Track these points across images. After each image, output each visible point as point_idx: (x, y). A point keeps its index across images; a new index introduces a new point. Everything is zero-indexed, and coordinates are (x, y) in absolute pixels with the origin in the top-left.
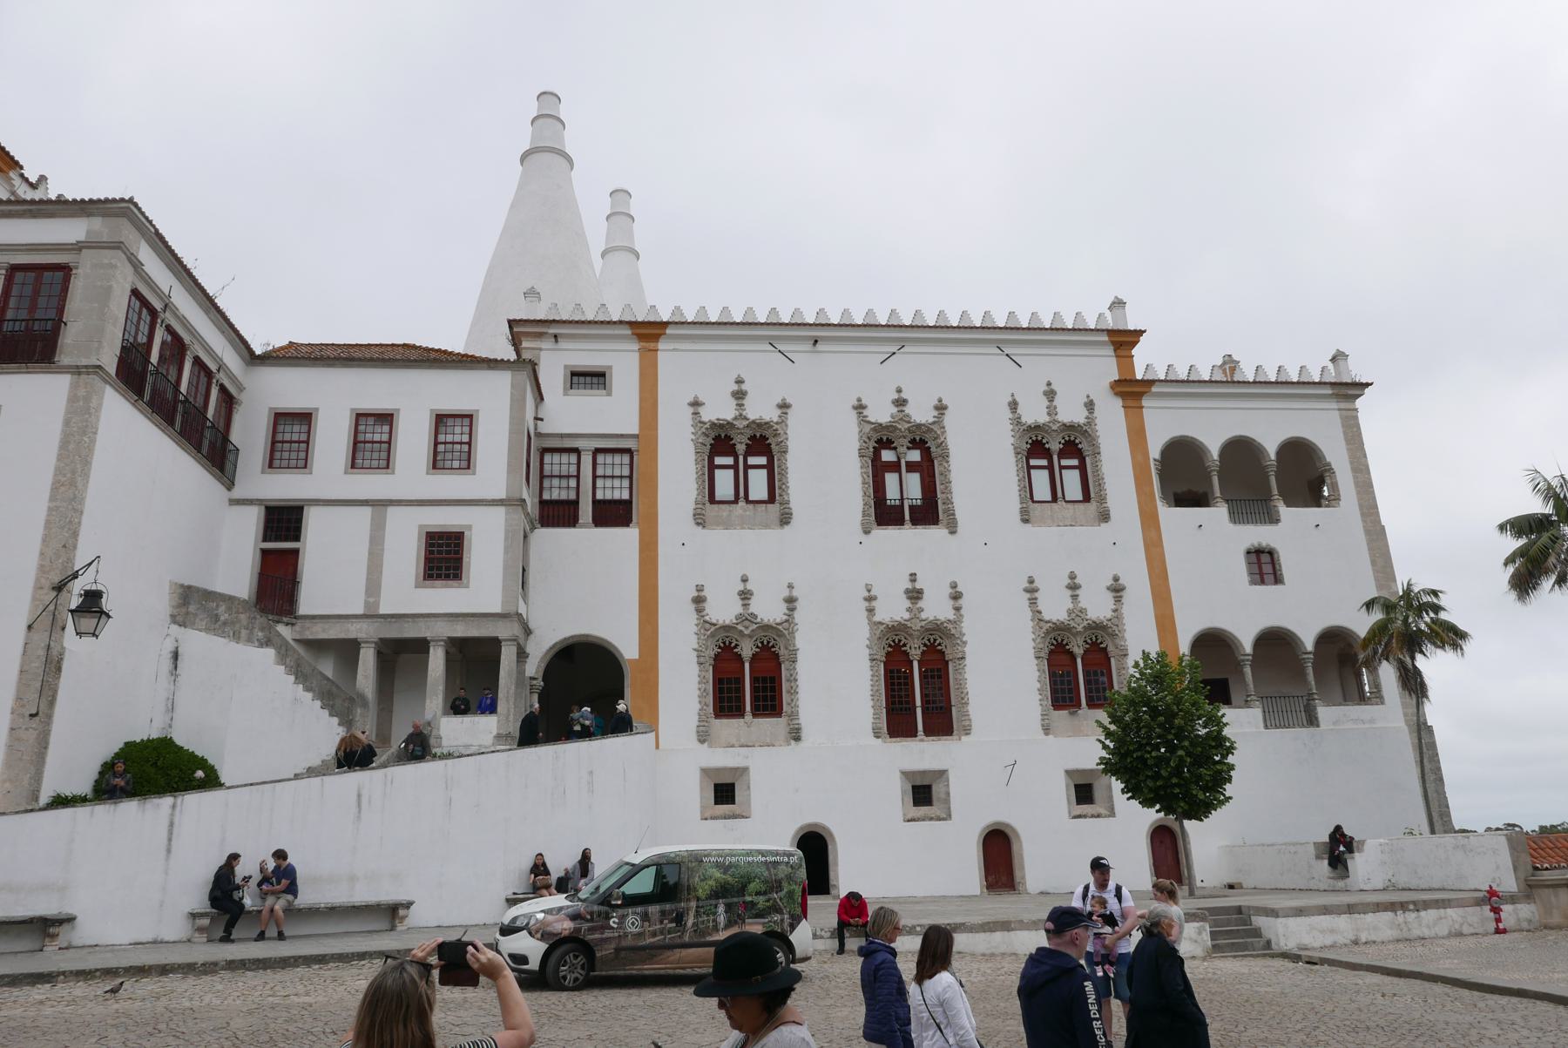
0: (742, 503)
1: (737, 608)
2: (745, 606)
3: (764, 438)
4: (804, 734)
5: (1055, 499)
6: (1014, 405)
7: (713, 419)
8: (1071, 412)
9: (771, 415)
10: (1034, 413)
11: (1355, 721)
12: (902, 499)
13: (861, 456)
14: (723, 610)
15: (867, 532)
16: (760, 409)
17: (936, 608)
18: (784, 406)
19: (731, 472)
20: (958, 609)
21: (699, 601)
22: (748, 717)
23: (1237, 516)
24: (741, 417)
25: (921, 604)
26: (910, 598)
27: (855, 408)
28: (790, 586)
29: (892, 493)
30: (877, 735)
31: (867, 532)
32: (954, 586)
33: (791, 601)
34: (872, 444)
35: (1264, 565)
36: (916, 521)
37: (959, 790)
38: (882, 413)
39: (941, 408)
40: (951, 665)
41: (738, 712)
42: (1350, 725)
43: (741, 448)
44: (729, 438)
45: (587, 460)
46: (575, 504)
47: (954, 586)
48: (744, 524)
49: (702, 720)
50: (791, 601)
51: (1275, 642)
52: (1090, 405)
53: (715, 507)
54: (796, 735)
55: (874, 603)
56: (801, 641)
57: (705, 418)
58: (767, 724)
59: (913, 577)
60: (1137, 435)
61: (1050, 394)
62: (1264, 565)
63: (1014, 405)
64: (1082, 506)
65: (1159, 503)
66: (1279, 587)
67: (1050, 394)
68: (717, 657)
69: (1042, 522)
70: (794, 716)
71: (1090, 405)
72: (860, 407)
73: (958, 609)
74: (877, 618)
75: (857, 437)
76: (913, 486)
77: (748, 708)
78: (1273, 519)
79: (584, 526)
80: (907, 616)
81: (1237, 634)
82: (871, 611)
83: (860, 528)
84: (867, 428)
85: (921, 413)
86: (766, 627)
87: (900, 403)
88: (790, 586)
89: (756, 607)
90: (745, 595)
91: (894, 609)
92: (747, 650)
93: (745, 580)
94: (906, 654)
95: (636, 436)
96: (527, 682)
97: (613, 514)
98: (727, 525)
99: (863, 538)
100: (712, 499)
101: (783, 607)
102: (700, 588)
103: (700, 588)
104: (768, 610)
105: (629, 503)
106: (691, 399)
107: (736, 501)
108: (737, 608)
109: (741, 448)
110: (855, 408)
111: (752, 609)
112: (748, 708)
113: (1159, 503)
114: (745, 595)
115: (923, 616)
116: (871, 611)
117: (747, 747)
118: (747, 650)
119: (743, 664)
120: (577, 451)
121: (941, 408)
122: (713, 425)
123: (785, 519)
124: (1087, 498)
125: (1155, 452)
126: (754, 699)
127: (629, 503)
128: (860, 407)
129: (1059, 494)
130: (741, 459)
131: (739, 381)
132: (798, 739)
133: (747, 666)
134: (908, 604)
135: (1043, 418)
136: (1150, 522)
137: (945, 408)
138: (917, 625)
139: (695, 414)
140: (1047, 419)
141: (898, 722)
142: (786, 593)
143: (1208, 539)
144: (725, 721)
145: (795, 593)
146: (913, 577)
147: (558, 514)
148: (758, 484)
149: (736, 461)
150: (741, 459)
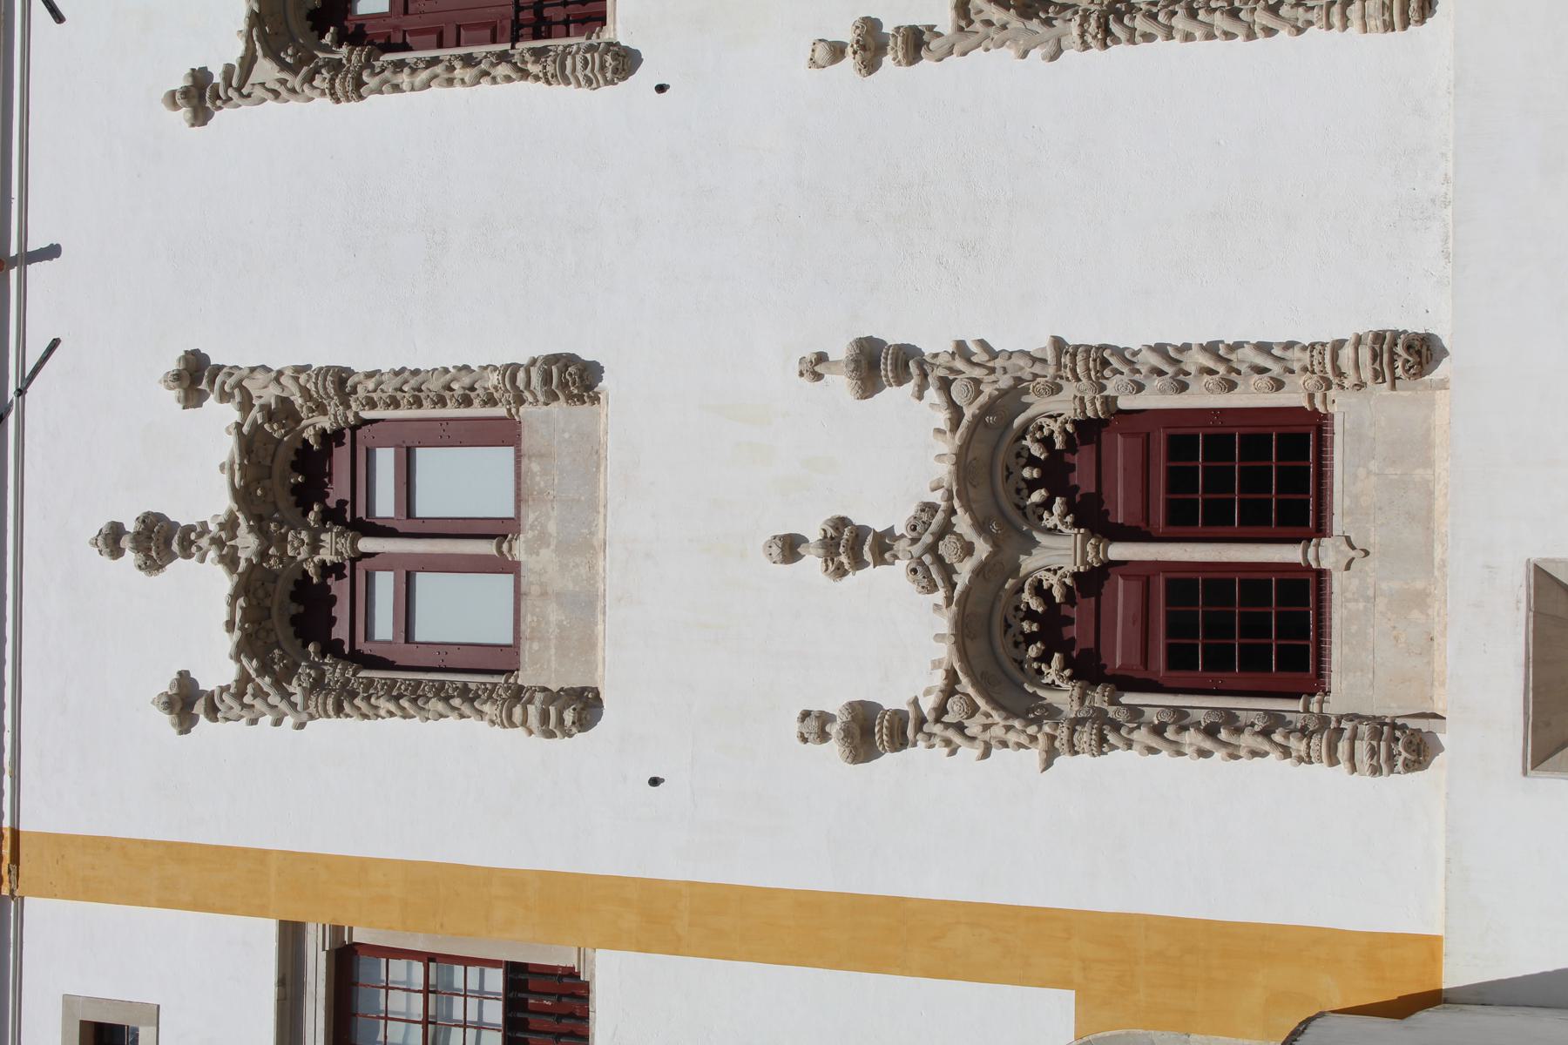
1: (890, 581)
2: (883, 546)
7: (228, 642)
9: (216, 427)
13: (358, 89)
14: (901, 637)
15: (625, 62)
19: (425, 583)
21: (869, 732)
22: (1328, 554)
27: (201, 116)
28: (816, 366)
31: (625, 62)
33: (875, 365)
41: (1303, 594)
48: (583, 546)
49: (1329, 735)
50: (875, 365)
53: (528, 650)
55: (888, 28)
56: (1020, 333)
58: (1352, 479)
68: (1088, 670)
70: (1327, 360)
72: (200, 96)
74: (945, 19)
75: (294, 105)
77: (1289, 554)
82: (916, 42)
83: (606, 93)
84: (266, 70)
86: (966, 467)
88: (816, 366)
89: (886, 508)
90: (850, 546)
92: (1057, 553)
93: (790, 548)
95: (291, 937)
98: (586, 604)
99: (643, 79)
101: (895, 397)
102: (816, 725)
103: (816, 725)
104: (902, 458)
105: (517, 974)
106: (165, 722)
107: (513, 568)
108: (890, 581)
110: (201, 116)
112: (1289, 554)
114: (850, 546)
116: (916, 42)
118: (1057, 553)
119: (1108, 568)
122: (245, 648)
123: (575, 379)
128: (200, 96)
131: (112, 539)
132: (1422, 353)
133: (1119, 551)
139: (212, 711)
142: (840, 384)
144: (1339, 653)
145: (840, 351)
148: (458, 482)
149: (389, 562)
150: (366, 544)
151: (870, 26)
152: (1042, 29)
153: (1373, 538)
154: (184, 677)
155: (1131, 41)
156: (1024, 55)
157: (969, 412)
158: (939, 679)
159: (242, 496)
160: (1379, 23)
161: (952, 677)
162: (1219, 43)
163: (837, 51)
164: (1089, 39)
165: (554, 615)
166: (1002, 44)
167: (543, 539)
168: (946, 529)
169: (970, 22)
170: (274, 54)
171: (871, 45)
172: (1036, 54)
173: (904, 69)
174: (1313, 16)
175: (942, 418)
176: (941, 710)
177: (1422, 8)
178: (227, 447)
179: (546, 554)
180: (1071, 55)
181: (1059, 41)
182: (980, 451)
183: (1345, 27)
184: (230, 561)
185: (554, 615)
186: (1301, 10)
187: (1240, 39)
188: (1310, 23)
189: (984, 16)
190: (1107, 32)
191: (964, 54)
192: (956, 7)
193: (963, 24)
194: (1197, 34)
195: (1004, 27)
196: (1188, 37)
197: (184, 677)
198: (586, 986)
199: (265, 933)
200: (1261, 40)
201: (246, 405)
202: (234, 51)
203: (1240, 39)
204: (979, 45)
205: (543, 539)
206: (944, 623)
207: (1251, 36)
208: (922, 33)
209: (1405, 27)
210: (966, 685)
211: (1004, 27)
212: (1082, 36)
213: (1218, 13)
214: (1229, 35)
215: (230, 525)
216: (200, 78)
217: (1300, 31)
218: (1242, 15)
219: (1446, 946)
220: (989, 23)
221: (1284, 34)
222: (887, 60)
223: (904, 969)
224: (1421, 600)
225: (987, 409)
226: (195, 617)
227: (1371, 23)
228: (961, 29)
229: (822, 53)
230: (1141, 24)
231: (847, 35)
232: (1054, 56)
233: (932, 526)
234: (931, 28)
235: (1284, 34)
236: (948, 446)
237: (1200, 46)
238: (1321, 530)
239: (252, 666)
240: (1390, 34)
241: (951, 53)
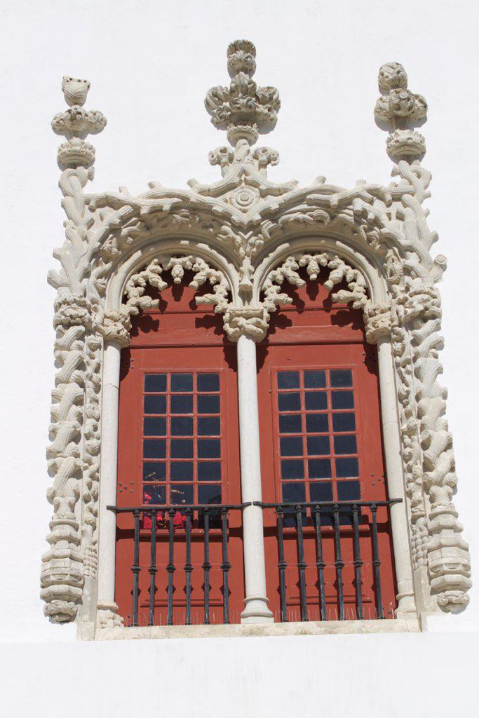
17: (324, 149)
20: (408, 154)
25: (264, 141)
26: (220, 123)
30: (63, 605)
32: (394, 82)
40: (385, 350)
47: (394, 82)
55: (90, 139)
59: (242, 56)
73: (408, 154)
74: (95, 189)
80: (213, 177)
82: (75, 161)
91: (163, 154)
94: (214, 320)
115: (274, 176)
116: (75, 161)
134: (221, 138)
151: (97, 125)
152: (78, 272)
155: (58, 347)
156: (56, 256)
160: (48, 572)
162: (47, 424)
163: (75, 99)
164: (64, 308)
166: (68, 237)
169: (92, 210)
172: (56, 266)
173: (55, 154)
174: (65, 509)
177: (60, 614)
180: (53, 295)
181: (67, 285)
183: (53, 541)
186: (72, 499)
187: (49, 444)
188: (57, 507)
189: (97, 220)
190: (67, 326)
191: (63, 206)
192: (107, 198)
193: (92, 203)
194: (57, 405)
195: (85, 239)
196: (56, 398)
200: (46, 464)
203: (49, 444)
204: (70, 218)
207: (51, 454)
208: (86, 165)
209: (43, 598)
211: (85, 239)
212: (65, 302)
213: (76, 422)
214: (53, 433)
217: (51, 498)
218: (73, 444)
220: (90, 224)
221: (51, 482)
222: (62, 140)
227: (49, 565)
228: (87, 202)
229: (75, 87)
230: (71, 357)
232: (52, 282)
234: (90, 177)
235: (51, 482)
237: (47, 407)
240: (39, 583)
241: (65, 194)
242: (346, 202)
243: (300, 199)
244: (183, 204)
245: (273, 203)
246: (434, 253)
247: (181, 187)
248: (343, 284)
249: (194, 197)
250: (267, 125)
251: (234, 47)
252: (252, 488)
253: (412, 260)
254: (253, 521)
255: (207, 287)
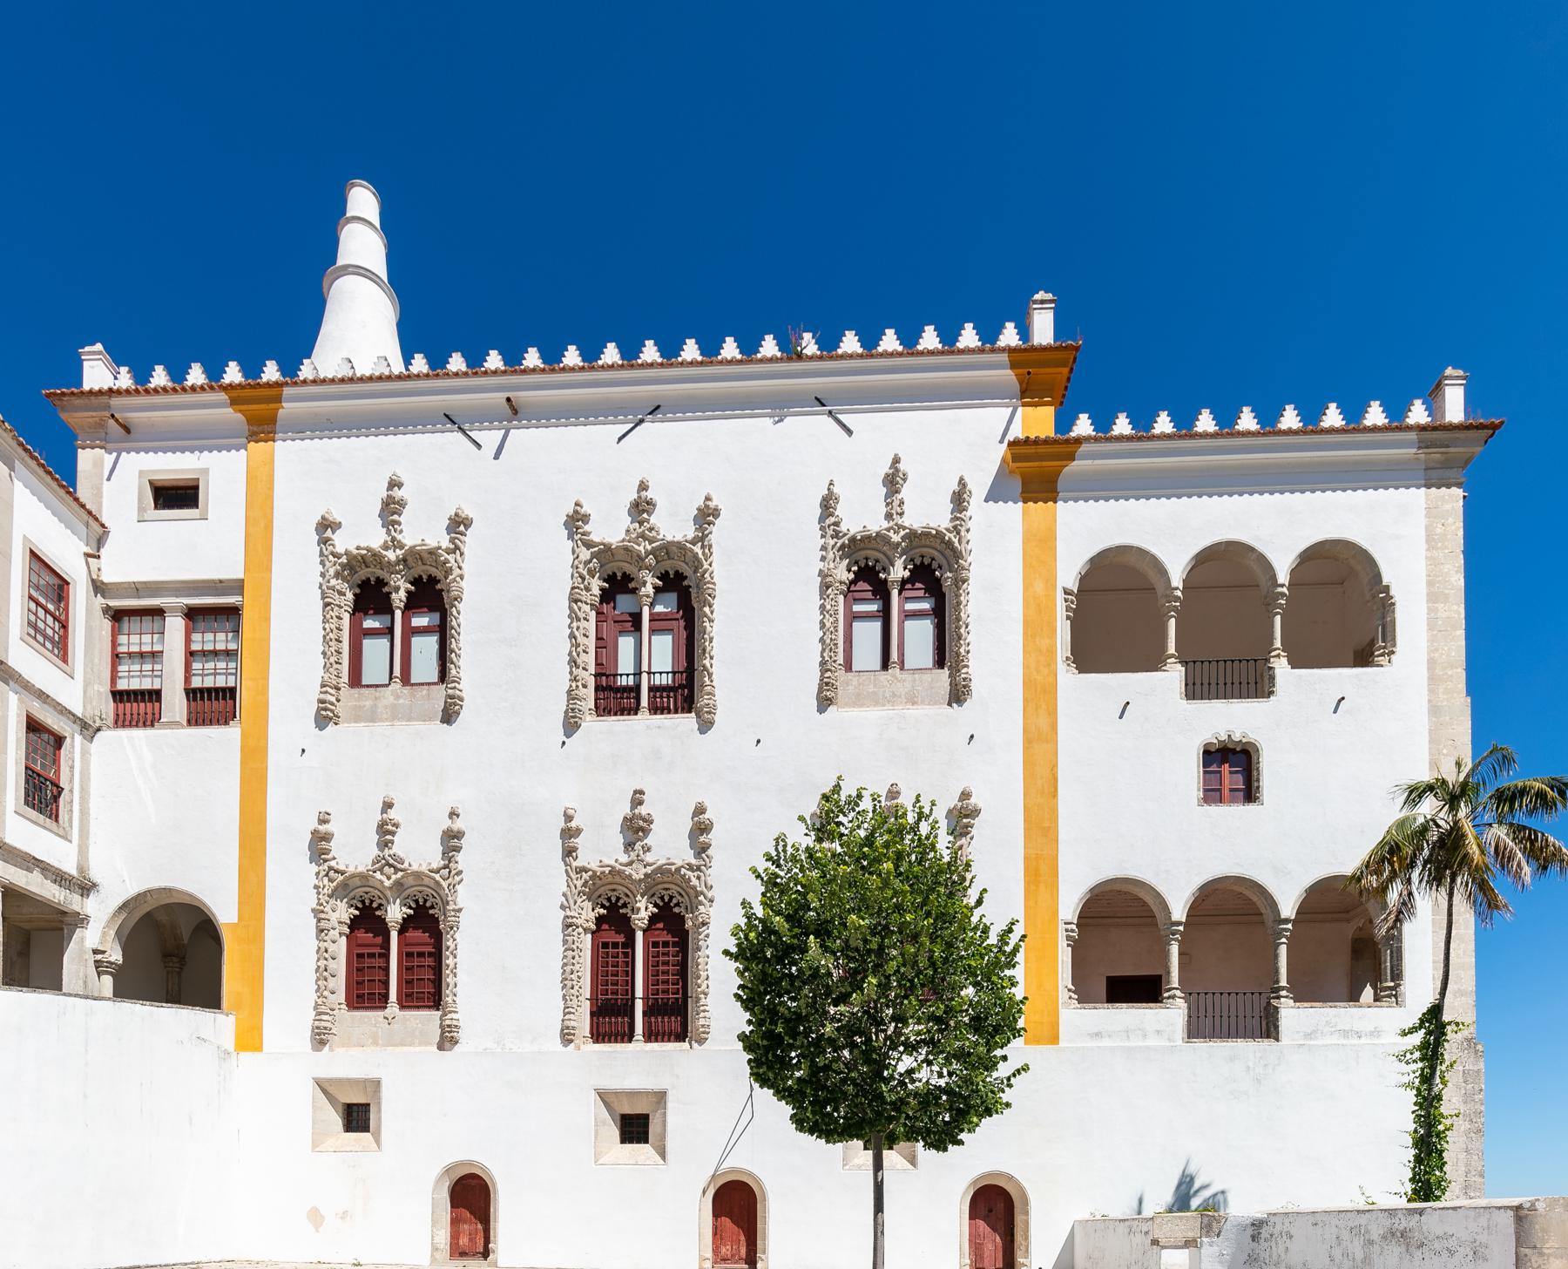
0: (397, 686)
3: (433, 580)
4: (462, 1035)
5: (886, 664)
6: (828, 504)
8: (925, 510)
9: (438, 538)
10: (863, 514)
11: (1345, 1033)
12: (638, 674)
14: (355, 852)
16: (422, 529)
18: (458, 524)
20: (701, 850)
23: (1196, 690)
24: (395, 544)
29: (625, 664)
30: (567, 1037)
33: (451, 841)
34: (596, 585)
35: (1232, 769)
36: (655, 709)
37: (676, 1123)
38: (611, 528)
39: (706, 516)
42: (1334, 1040)
43: (399, 598)
44: (381, 583)
45: (175, 625)
46: (155, 695)
47: (700, 810)
48: (396, 715)
50: (451, 841)
51: (1231, 906)
52: (959, 500)
53: (356, 691)
54: (447, 1040)
57: (340, 549)
59: (637, 799)
60: (1040, 547)
61: (893, 482)
62: (1232, 769)
63: (828, 504)
64: (927, 677)
65: (1061, 667)
66: (1251, 807)
67: (893, 482)
69: (858, 701)
71: (959, 500)
72: (576, 521)
76: (661, 654)
78: (1258, 685)
79: (173, 724)
81: (1161, 888)
82: (569, 852)
84: (585, 554)
85: (673, 525)
87: (641, 508)
89: (400, 846)
90: (386, 832)
91: (603, 849)
96: (91, 958)
97: (213, 705)
100: (356, 680)
104: (418, 850)
105: (232, 691)
109: (399, 598)
111: (395, 849)
113: (1061, 667)
114: (386, 832)
115: (649, 858)
117: (387, 1049)
120: (158, 612)
121: (706, 516)
124: (940, 662)
125: (1068, 575)
126: (405, 982)
127: (232, 691)
129: (894, 656)
130: (398, 614)
135: (875, 522)
136: (1040, 699)
137: (716, 513)
138: (638, 873)
140: (885, 525)
141: (610, 1019)
143: (1155, 719)
145: (458, 824)
146: (637, 799)
147: (136, 707)
150: (398, 614)
151: (578, 831)
153: (395, 1026)
154: (339, 525)
157: (437, 877)
158: (342, 867)
159: (412, 550)
161: (343, 873)
163: (569, 818)
165: (368, 703)
167: (398, 697)
168: (397, 870)
170: (594, 556)
171: (569, 834)
175: (435, 866)
176: (331, 868)
178: (432, 543)
179: (391, 699)
182: (427, 881)
184: (386, 548)
185: (368, 703)
197: (339, 525)
198: (226, 723)
199: (238, 573)
201: (449, 552)
202: (595, 538)
205: (398, 697)
206: (361, 869)
210: (341, 878)
215: (402, 547)
216: (585, 519)
219: (257, 1054)
223: (241, 858)
224: (375, 1043)
225: (437, 883)
226: (362, 533)
231: (573, 824)
233: (394, 864)
236: (424, 869)
238: (402, 1007)
239: (344, 560)
242: (678, 870)
243: (660, 867)
244: (613, 872)
245: (649, 870)
246: (709, 895)
247: (612, 863)
248: (678, 905)
249: (618, 867)
250: (646, 832)
251: (636, 792)
252: (639, 992)
253: (701, 898)
254: (639, 1006)
255: (625, 905)
